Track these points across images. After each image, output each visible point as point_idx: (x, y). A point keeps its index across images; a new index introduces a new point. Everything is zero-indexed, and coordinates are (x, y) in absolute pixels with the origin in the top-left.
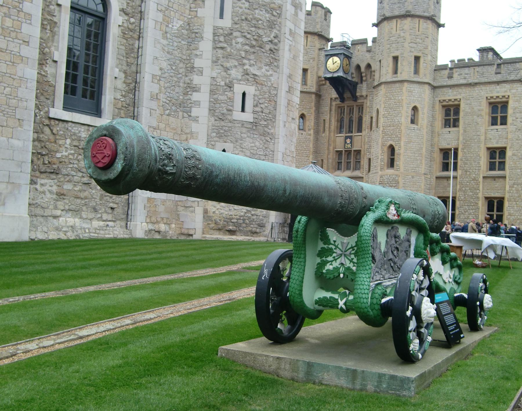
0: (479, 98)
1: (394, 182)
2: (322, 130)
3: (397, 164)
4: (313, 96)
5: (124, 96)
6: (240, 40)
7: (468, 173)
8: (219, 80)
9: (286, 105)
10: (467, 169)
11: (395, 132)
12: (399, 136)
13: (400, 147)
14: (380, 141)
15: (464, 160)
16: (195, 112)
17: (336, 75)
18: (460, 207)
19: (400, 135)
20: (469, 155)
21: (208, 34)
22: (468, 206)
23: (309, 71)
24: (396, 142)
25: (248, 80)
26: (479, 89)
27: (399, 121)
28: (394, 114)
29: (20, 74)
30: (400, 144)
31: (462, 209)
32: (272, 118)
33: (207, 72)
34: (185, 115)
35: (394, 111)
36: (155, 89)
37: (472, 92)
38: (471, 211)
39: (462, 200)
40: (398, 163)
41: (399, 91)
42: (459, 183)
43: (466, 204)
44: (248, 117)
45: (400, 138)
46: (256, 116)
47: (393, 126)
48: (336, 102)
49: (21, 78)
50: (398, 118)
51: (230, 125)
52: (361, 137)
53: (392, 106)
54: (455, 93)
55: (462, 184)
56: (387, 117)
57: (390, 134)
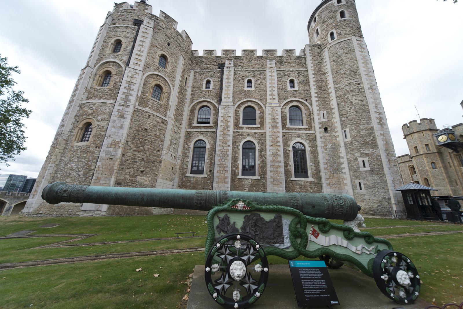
2: (449, 167)
4: (437, 154)
5: (315, 170)
6: (356, 143)
8: (351, 158)
9: (388, 161)
16: (344, 171)
17: (446, 143)
21: (342, 145)
23: (429, 145)
25: (364, 156)
29: (279, 170)
32: (381, 167)
33: (345, 157)
34: (340, 172)
36: (326, 166)
44: (368, 168)
46: (371, 168)
49: (280, 171)
51: (360, 173)
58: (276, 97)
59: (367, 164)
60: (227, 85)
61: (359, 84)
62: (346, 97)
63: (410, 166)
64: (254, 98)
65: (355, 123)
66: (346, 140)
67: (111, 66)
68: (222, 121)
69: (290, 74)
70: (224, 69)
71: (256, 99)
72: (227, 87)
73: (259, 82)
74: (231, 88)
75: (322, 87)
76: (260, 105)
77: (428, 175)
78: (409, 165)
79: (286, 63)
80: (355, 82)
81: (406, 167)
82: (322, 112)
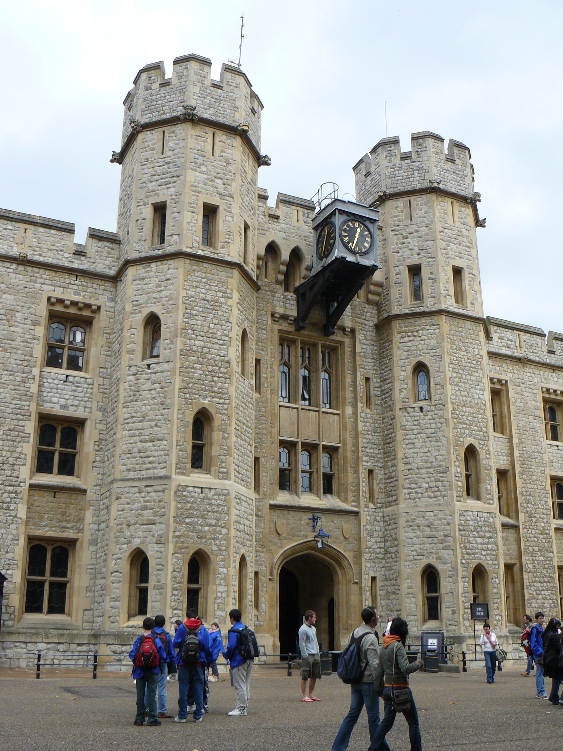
0: (533, 387)
1: (487, 529)
3: (486, 489)
7: (534, 520)
10: (531, 513)
11: (476, 419)
12: (484, 429)
13: (488, 452)
14: (451, 435)
15: (525, 493)
18: (530, 586)
19: (486, 427)
20: (531, 486)
22: (540, 582)
24: (481, 442)
26: (531, 371)
27: (480, 398)
28: (470, 382)
30: (487, 446)
31: (532, 588)
35: (469, 374)
37: (522, 373)
38: (546, 593)
39: (530, 572)
40: (489, 487)
41: (474, 337)
42: (523, 537)
43: (537, 579)
45: (485, 434)
47: (470, 407)
48: (281, 325)
50: (478, 391)
52: (336, 417)
53: (464, 364)
54: (498, 368)
55: (528, 541)
56: (457, 385)
57: (468, 422)
63: (60, 301)
77: (221, 394)
78: (59, 293)
81: (33, 296)
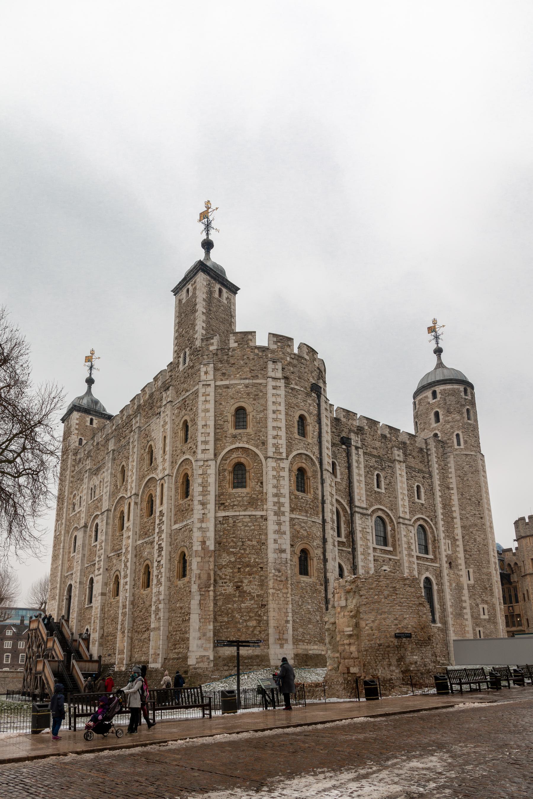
6: (478, 588)
32: (495, 616)
58: (407, 510)
59: (486, 611)
60: (358, 478)
61: (481, 518)
62: (471, 530)
64: (384, 505)
65: (478, 564)
66: (469, 582)
67: (304, 461)
68: (361, 538)
69: (416, 476)
70: (350, 447)
71: (386, 507)
72: (359, 481)
73: (388, 481)
74: (363, 485)
75: (447, 505)
76: (391, 518)
79: (410, 457)
80: (479, 514)
82: (447, 541)
